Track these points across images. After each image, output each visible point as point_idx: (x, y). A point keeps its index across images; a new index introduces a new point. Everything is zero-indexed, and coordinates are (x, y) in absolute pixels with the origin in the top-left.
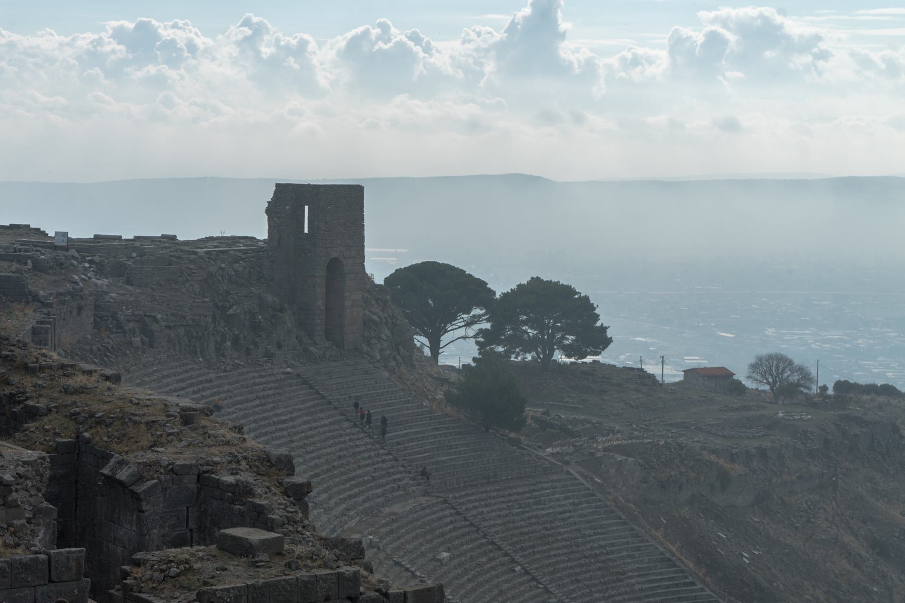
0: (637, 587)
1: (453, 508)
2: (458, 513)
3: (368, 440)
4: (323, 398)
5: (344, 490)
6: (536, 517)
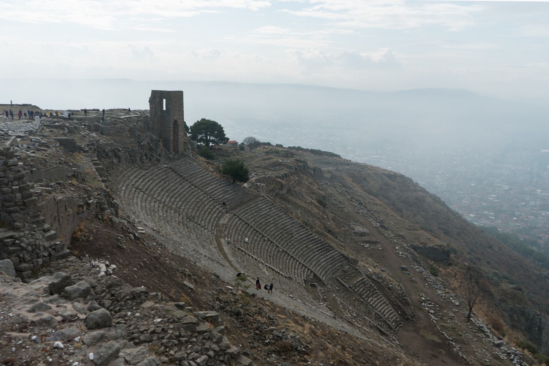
0: (298, 238)
3: (203, 193)
4: (181, 176)
6: (261, 215)
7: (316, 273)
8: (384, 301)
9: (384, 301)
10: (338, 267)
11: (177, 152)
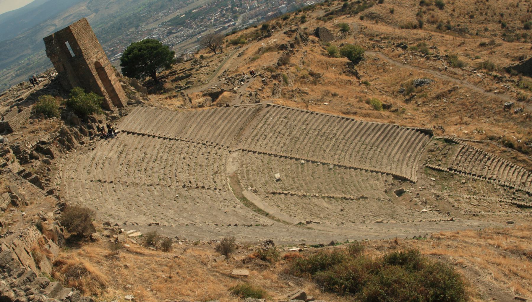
7: (394, 173)
8: (505, 164)
9: (505, 164)
11: (119, 105)
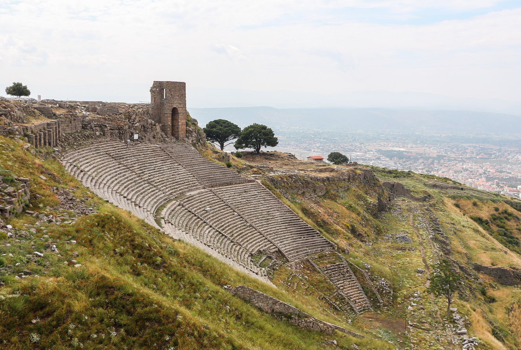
1: (213, 193)
2: (215, 195)
5: (173, 186)
10: (316, 251)
